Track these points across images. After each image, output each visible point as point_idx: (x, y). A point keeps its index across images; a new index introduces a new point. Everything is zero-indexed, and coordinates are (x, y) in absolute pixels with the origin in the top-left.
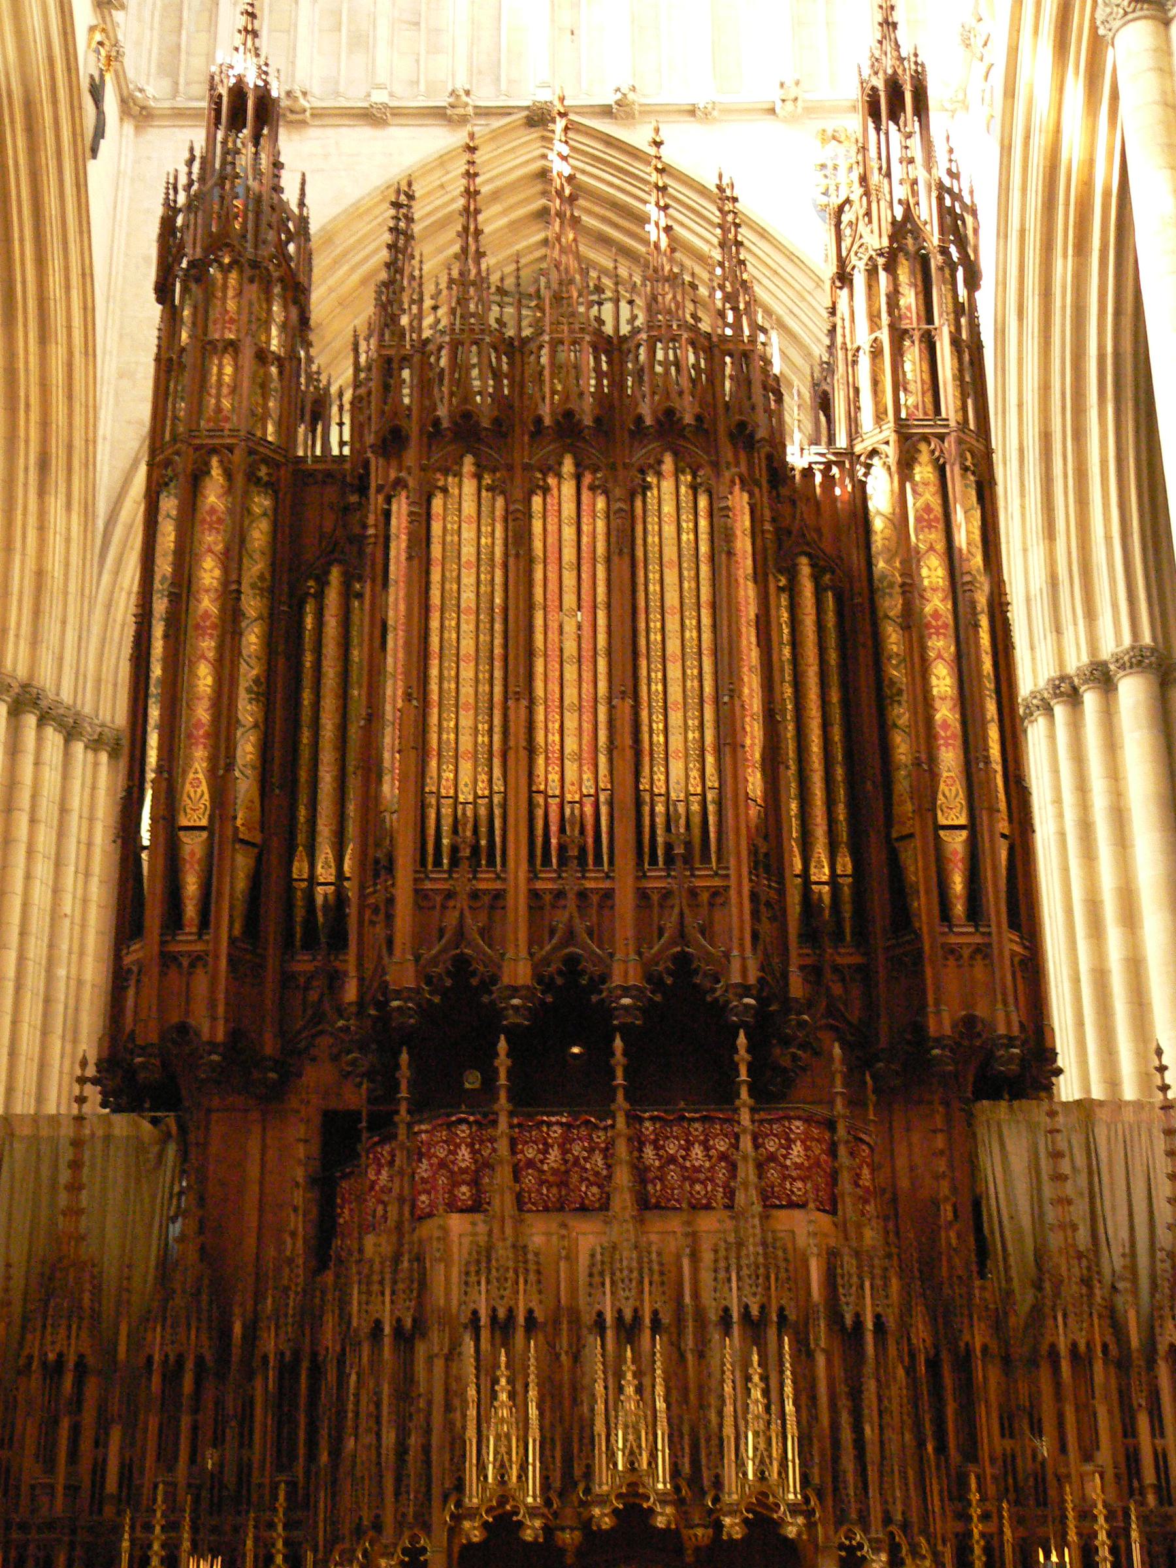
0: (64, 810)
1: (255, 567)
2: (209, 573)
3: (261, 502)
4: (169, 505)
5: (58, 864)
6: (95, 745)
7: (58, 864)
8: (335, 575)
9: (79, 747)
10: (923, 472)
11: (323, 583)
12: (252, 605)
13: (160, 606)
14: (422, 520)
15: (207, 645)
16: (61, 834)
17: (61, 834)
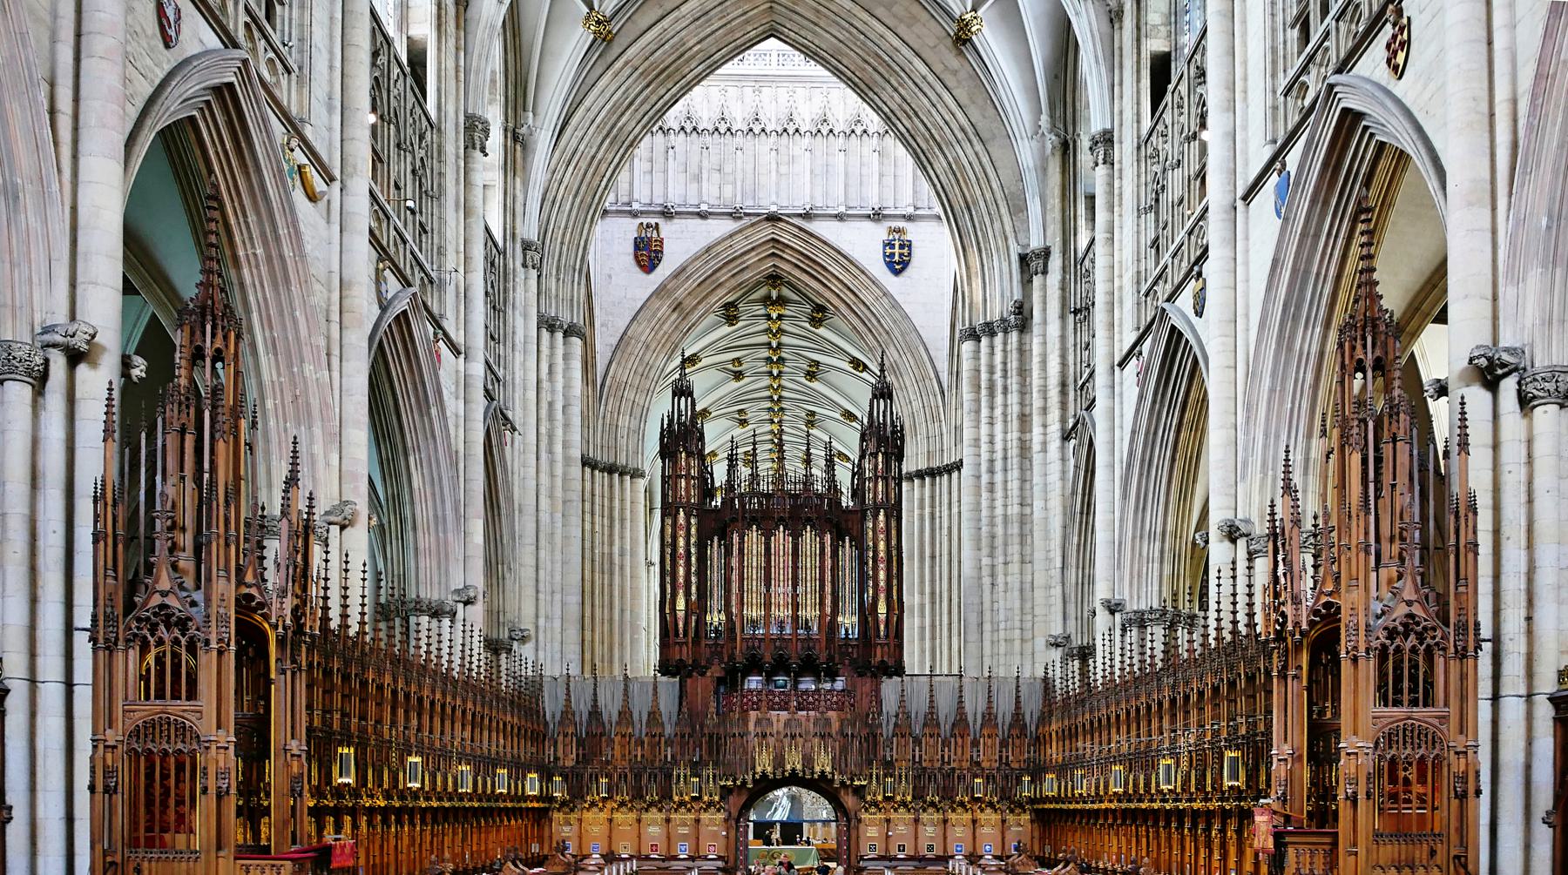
0: (593, 495)
1: (693, 540)
2: (681, 542)
3: (693, 521)
4: (669, 521)
5: (593, 514)
6: (602, 471)
7: (593, 514)
8: (716, 539)
9: (597, 472)
10: (881, 517)
11: (712, 541)
12: (693, 550)
13: (669, 550)
14: (742, 542)
15: (681, 562)
16: (593, 504)
17: (593, 504)
